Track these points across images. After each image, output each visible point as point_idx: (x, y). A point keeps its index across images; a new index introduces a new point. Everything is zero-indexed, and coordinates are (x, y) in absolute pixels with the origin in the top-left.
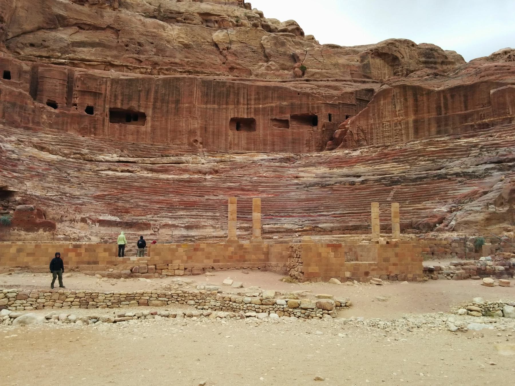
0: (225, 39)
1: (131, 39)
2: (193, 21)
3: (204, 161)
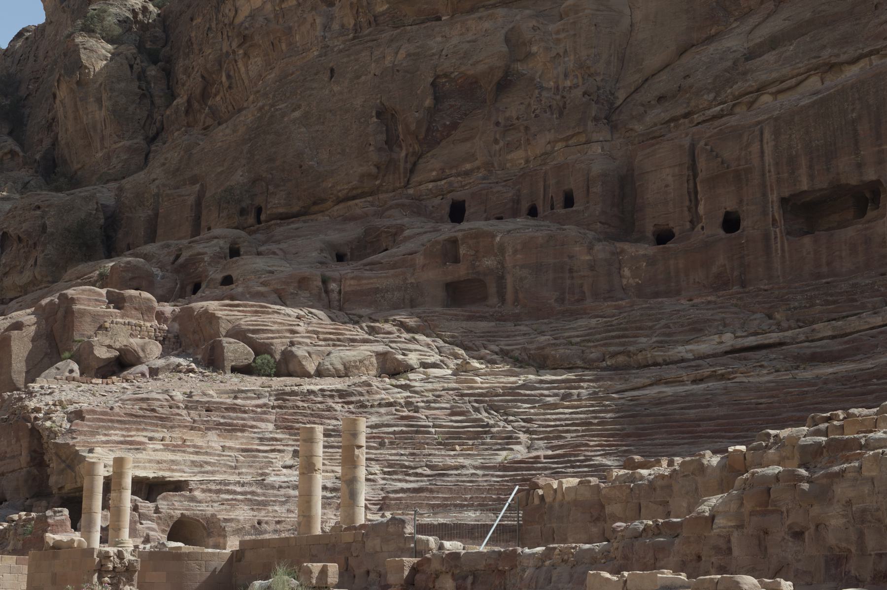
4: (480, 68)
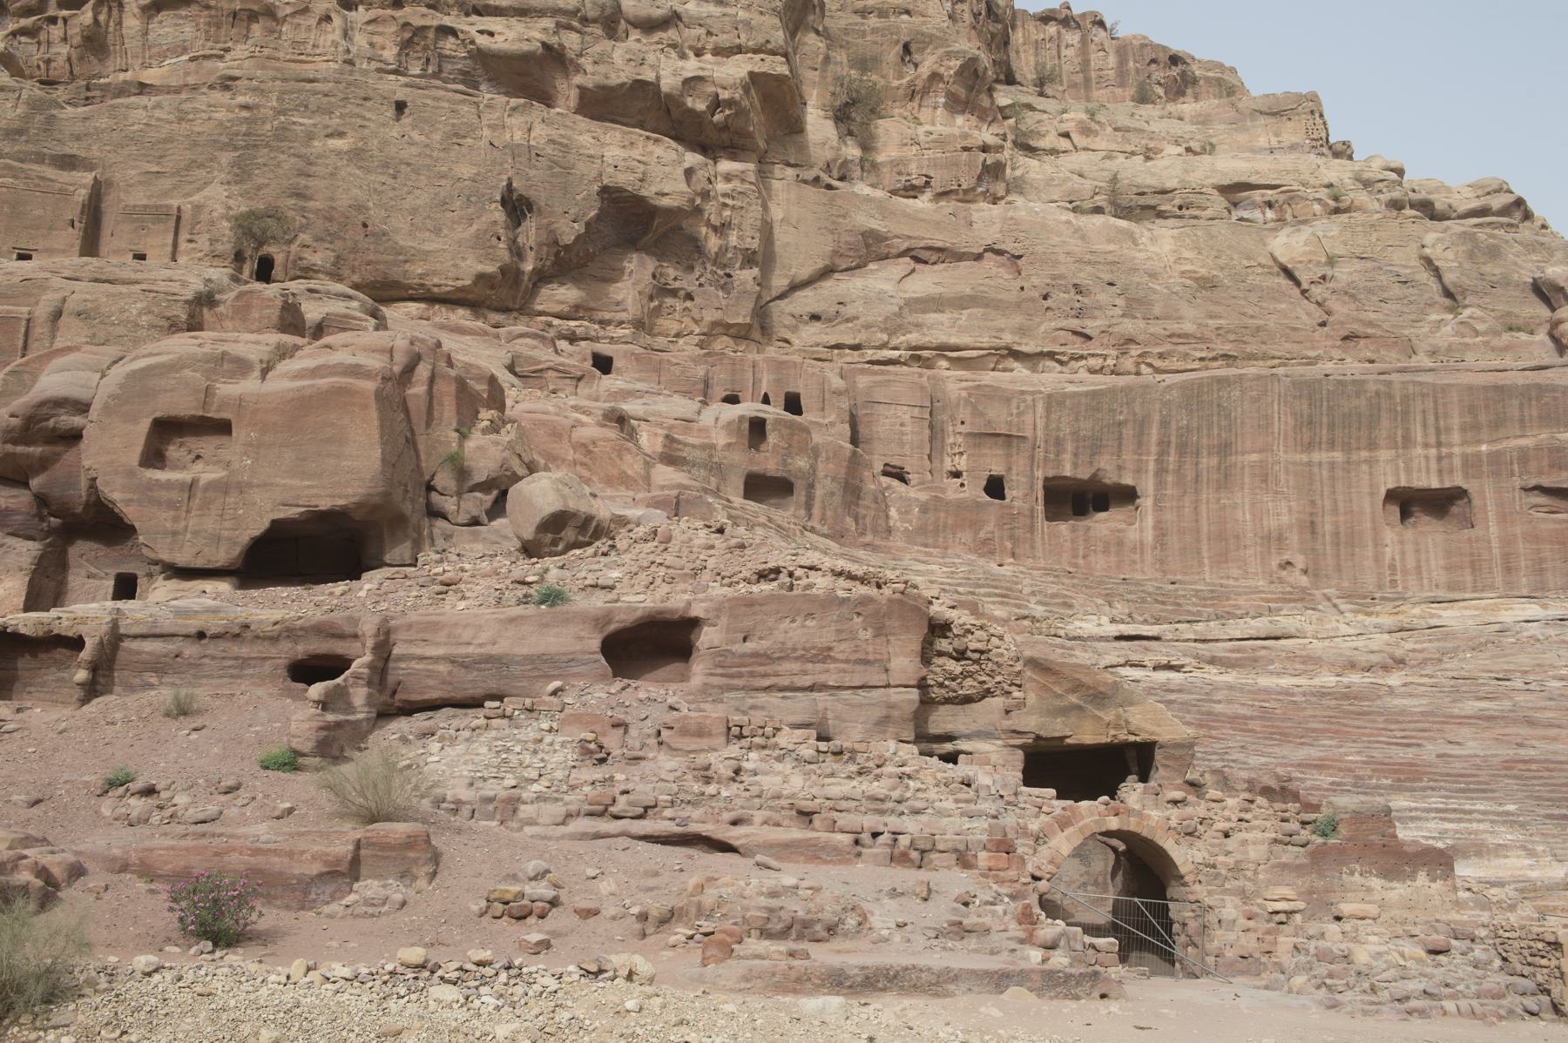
0: (1311, 253)
1: (1054, 277)
2: (1206, 209)
3: (1340, 632)
4: (665, 202)
